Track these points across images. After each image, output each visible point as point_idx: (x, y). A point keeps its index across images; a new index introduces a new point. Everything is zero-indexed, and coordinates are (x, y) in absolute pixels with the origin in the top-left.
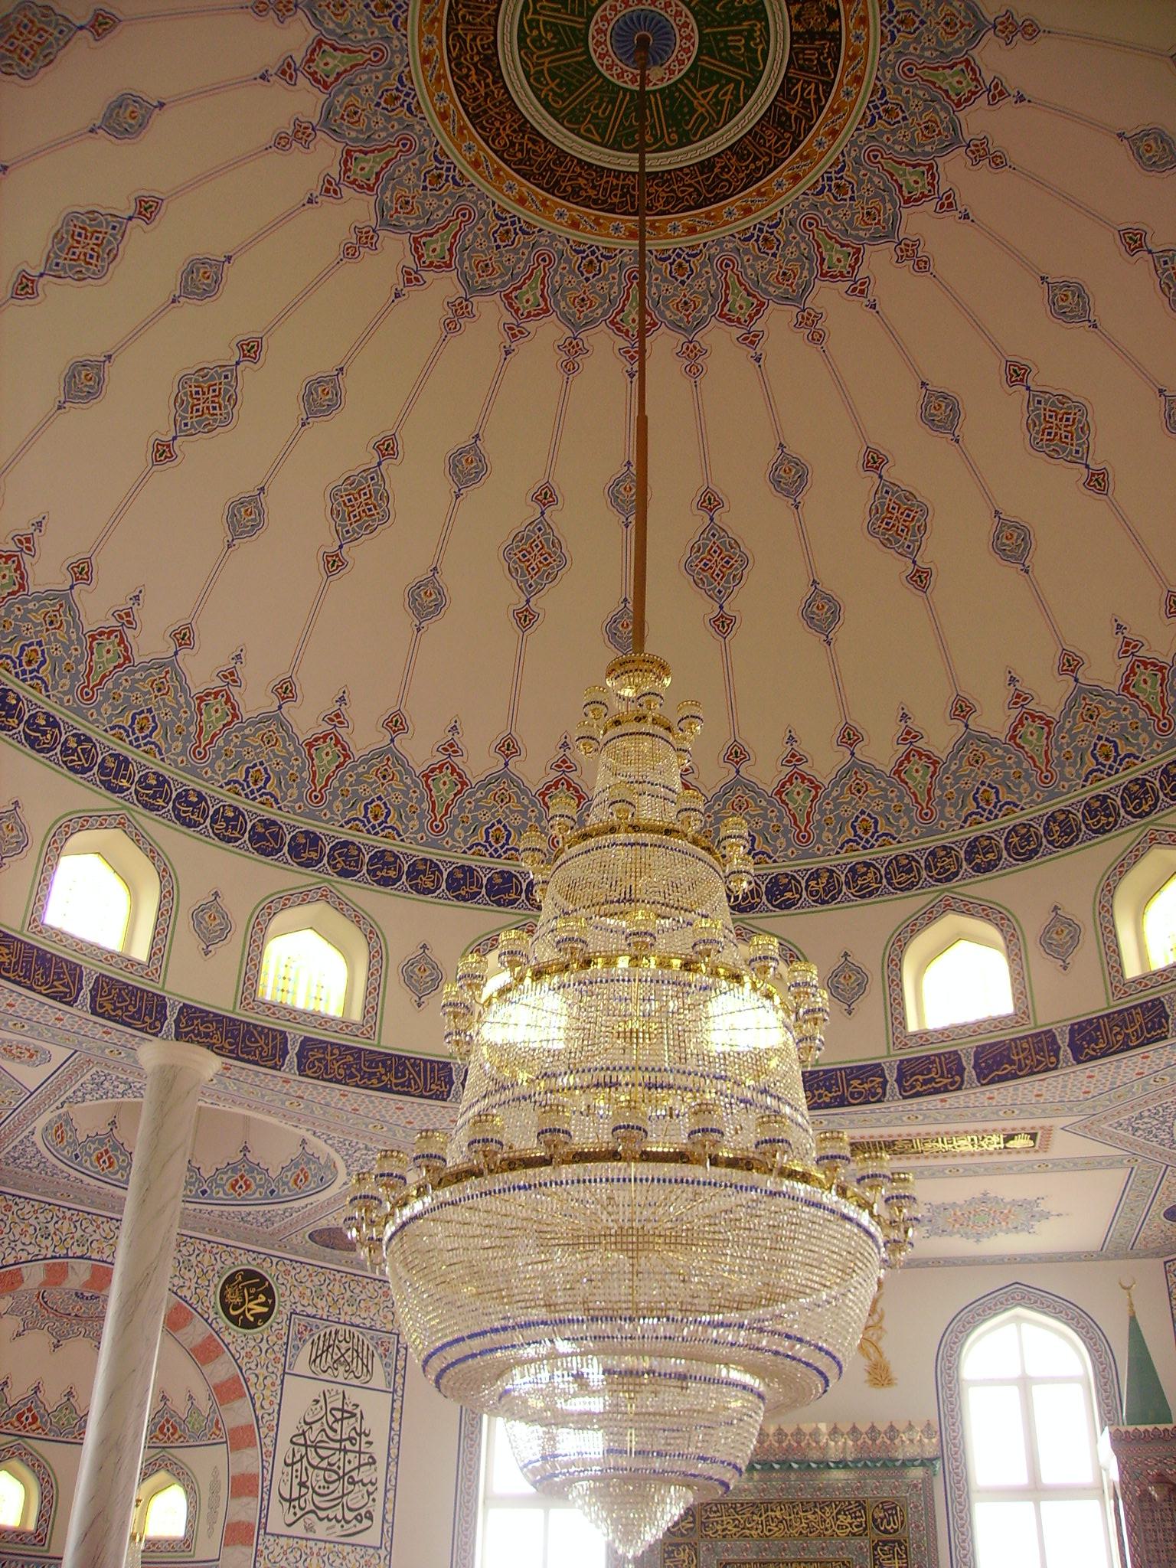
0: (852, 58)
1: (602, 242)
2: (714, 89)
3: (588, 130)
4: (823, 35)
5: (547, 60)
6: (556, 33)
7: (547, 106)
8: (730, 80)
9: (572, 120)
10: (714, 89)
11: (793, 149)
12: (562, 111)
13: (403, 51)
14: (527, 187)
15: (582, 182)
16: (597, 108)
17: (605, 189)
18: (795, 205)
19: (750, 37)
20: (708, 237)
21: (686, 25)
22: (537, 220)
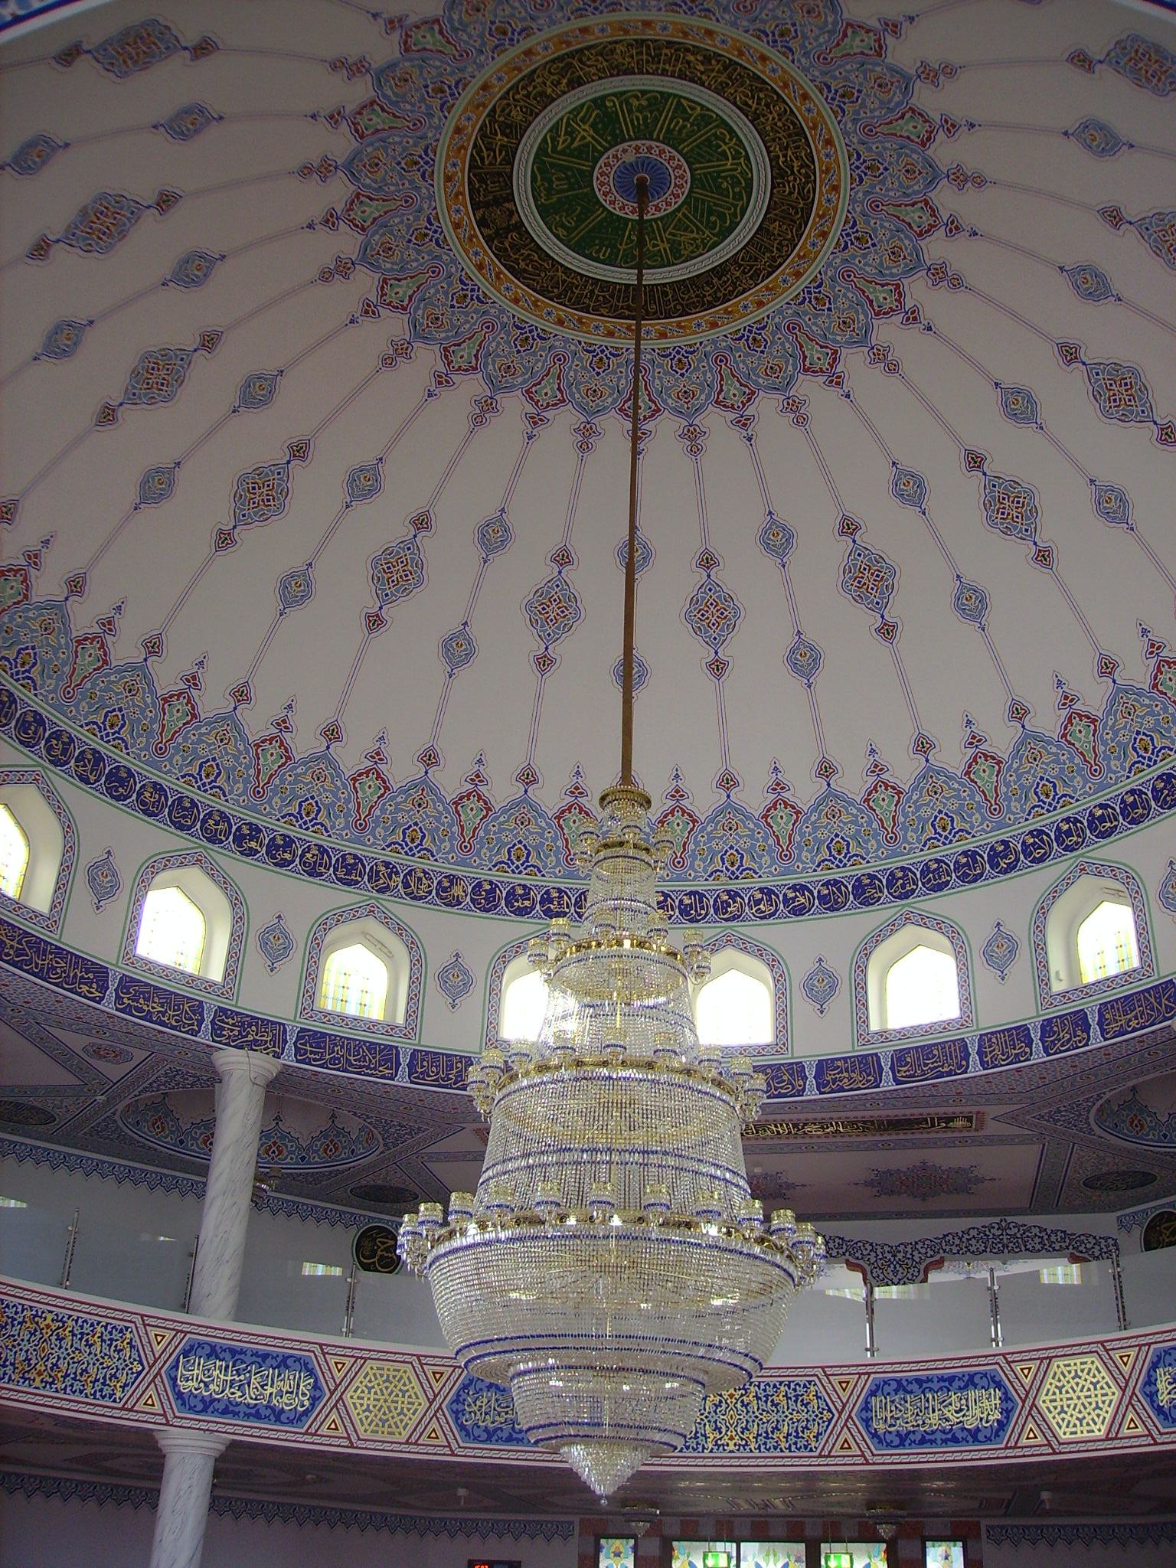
2: (576, 144)
3: (693, 109)
4: (487, 205)
5: (728, 167)
6: (719, 186)
7: (731, 131)
9: (707, 118)
10: (576, 144)
11: (494, 110)
12: (717, 126)
13: (853, 201)
14: (757, 69)
15: (702, 68)
17: (677, 60)
18: (481, 66)
20: (566, 27)
21: (605, 194)
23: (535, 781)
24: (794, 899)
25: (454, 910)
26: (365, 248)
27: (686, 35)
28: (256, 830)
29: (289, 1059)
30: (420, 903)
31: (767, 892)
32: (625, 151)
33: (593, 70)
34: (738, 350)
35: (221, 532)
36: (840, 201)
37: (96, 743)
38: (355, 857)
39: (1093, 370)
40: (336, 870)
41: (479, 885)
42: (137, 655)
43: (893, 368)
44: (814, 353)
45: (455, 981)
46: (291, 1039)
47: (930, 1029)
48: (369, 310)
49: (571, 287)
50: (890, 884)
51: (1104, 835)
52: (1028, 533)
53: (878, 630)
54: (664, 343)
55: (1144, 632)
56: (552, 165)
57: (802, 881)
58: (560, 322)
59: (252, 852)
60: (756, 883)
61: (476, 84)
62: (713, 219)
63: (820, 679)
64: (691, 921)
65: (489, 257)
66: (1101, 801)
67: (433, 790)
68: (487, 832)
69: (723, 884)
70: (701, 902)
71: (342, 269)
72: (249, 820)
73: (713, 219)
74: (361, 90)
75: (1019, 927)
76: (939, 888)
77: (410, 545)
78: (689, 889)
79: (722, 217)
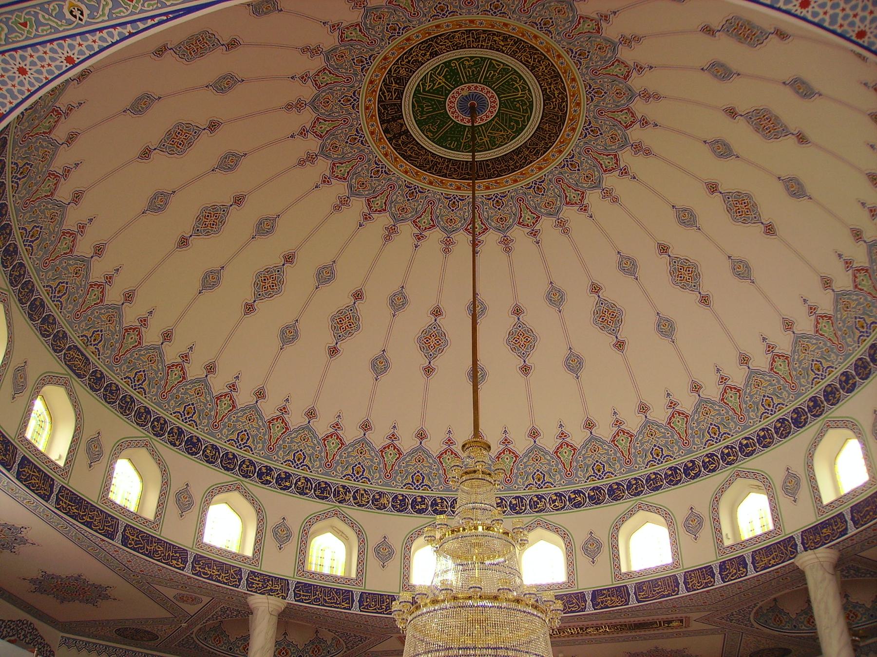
0: (373, 116)
1: (490, 18)
4: (388, 121)
7: (520, 77)
8: (428, 91)
9: (506, 70)
13: (588, 110)
14: (533, 43)
16: (494, 75)
18: (383, 47)
19: (422, 113)
20: (427, 25)
21: (453, 113)
22: (528, 28)
23: (426, 437)
24: (574, 499)
25: (382, 511)
26: (322, 147)
27: (493, 26)
28: (269, 470)
29: (291, 600)
30: (363, 508)
31: (559, 495)
32: (462, 89)
33: (444, 47)
34: (529, 194)
35: (247, 304)
36: (581, 111)
37: (180, 424)
38: (326, 483)
39: (726, 196)
40: (315, 491)
41: (396, 497)
42: (202, 373)
43: (615, 200)
44: (571, 194)
45: (384, 552)
46: (292, 588)
47: (656, 570)
48: (326, 180)
49: (436, 164)
50: (629, 488)
51: (748, 455)
52: (696, 288)
53: (615, 345)
54: (488, 192)
55: (764, 339)
56: (423, 99)
57: (579, 488)
58: (431, 183)
59: (267, 482)
60: (553, 490)
61: (380, 58)
62: (512, 124)
63: (583, 374)
64: (517, 513)
65: (390, 149)
66: (746, 435)
67: (368, 444)
68: (399, 467)
69: (533, 492)
70: (522, 502)
71: (311, 158)
72: (266, 464)
73: (512, 124)
74: (318, 63)
75: (703, 510)
76: (657, 489)
77: (352, 308)
78: (515, 495)
79: (517, 122)
